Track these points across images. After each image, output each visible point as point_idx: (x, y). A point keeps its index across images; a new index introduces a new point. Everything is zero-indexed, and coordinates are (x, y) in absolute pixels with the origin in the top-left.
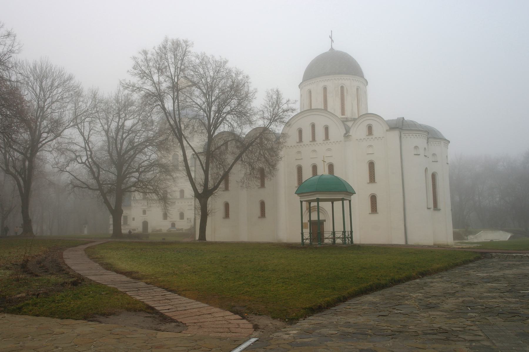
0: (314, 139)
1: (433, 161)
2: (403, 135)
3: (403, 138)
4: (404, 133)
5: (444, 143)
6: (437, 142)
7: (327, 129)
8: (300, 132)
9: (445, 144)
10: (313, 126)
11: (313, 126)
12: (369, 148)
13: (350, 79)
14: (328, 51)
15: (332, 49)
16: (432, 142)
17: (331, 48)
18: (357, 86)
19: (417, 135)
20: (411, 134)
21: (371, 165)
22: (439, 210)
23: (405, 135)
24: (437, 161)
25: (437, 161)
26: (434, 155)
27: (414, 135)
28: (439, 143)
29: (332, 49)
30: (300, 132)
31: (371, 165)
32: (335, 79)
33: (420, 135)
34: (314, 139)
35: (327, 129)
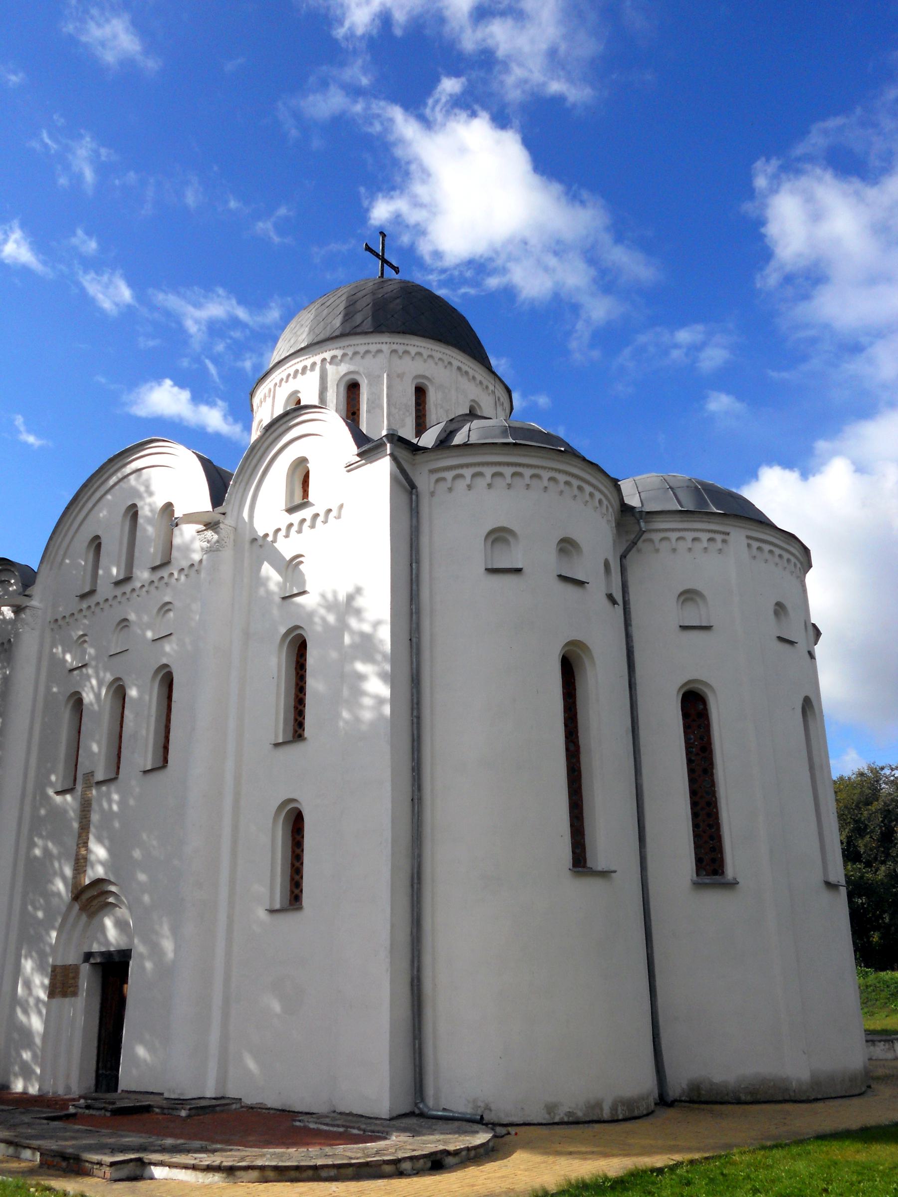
1: (680, 626)
2: (423, 481)
3: (432, 494)
4: (432, 471)
5: (748, 537)
6: (704, 536)
9: (755, 544)
13: (380, 351)
16: (674, 536)
18: (416, 377)
19: (508, 471)
20: (468, 472)
22: (732, 885)
23: (444, 479)
24: (708, 628)
25: (708, 628)
26: (689, 596)
27: (488, 471)
28: (719, 537)
33: (527, 472)
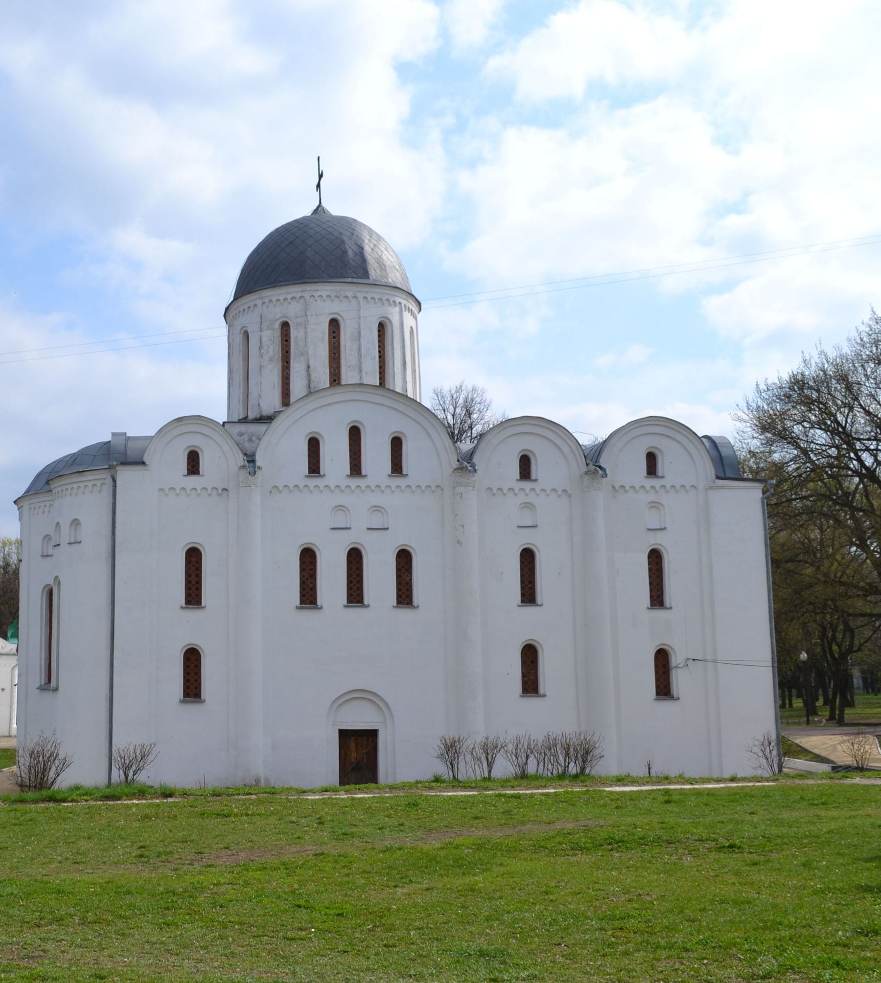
0: (356, 468)
7: (397, 444)
8: (314, 445)
10: (355, 434)
11: (355, 434)
12: (523, 508)
14: (309, 214)
15: (319, 209)
17: (318, 203)
21: (528, 557)
29: (319, 209)
30: (314, 445)
31: (528, 557)
32: (380, 299)
34: (356, 468)
35: (397, 444)
